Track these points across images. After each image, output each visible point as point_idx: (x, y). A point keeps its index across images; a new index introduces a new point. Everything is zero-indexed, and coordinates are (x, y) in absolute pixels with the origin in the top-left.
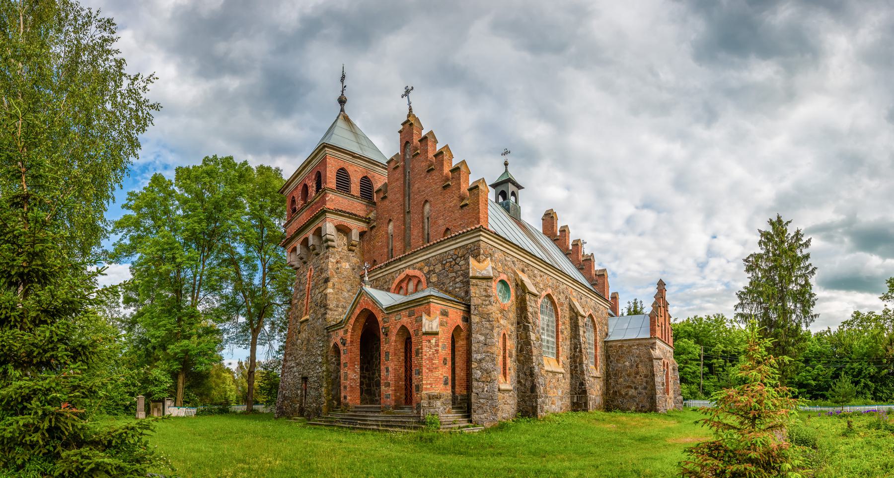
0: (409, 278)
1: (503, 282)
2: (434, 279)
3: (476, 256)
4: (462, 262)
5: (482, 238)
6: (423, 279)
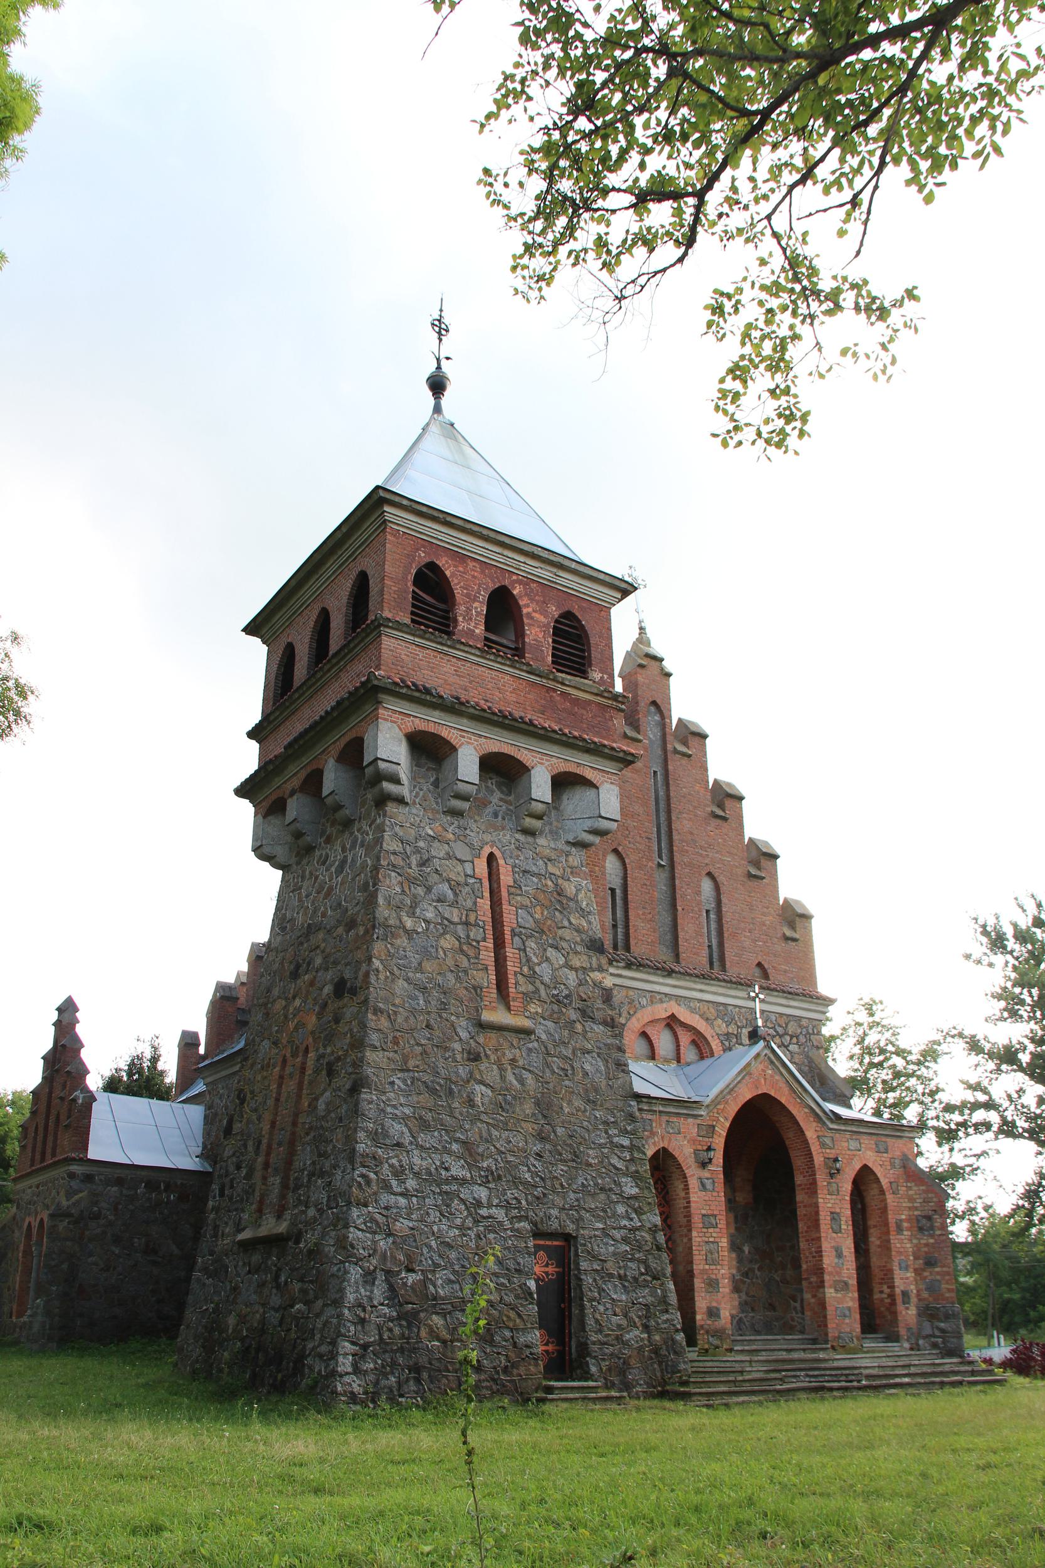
0: (672, 1023)
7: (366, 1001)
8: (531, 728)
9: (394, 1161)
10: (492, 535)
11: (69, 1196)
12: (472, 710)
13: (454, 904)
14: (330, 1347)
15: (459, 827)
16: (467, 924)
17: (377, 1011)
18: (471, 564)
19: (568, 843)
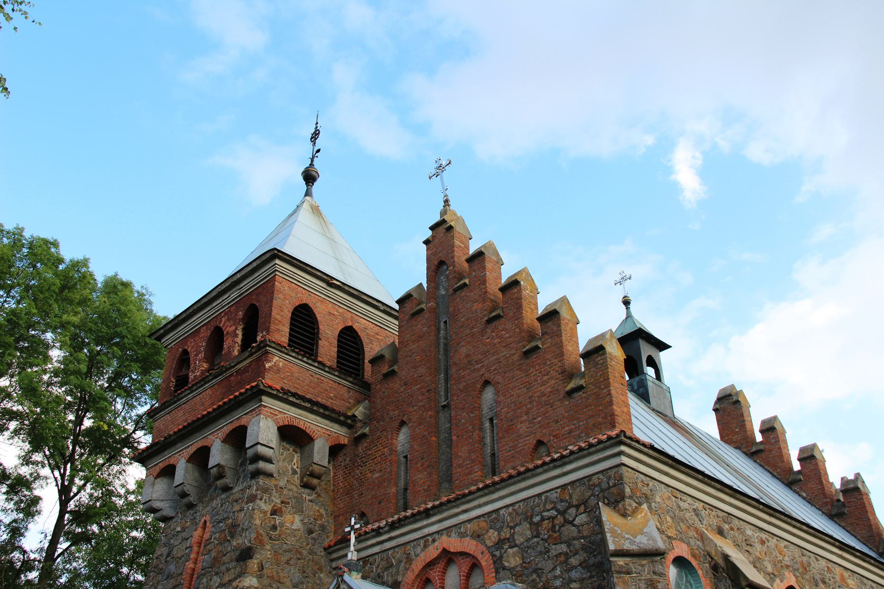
0: (448, 557)
1: (680, 562)
2: (513, 559)
3: (616, 501)
4: (582, 519)
5: (625, 460)
6: (485, 561)
8: (201, 421)
10: (198, 305)
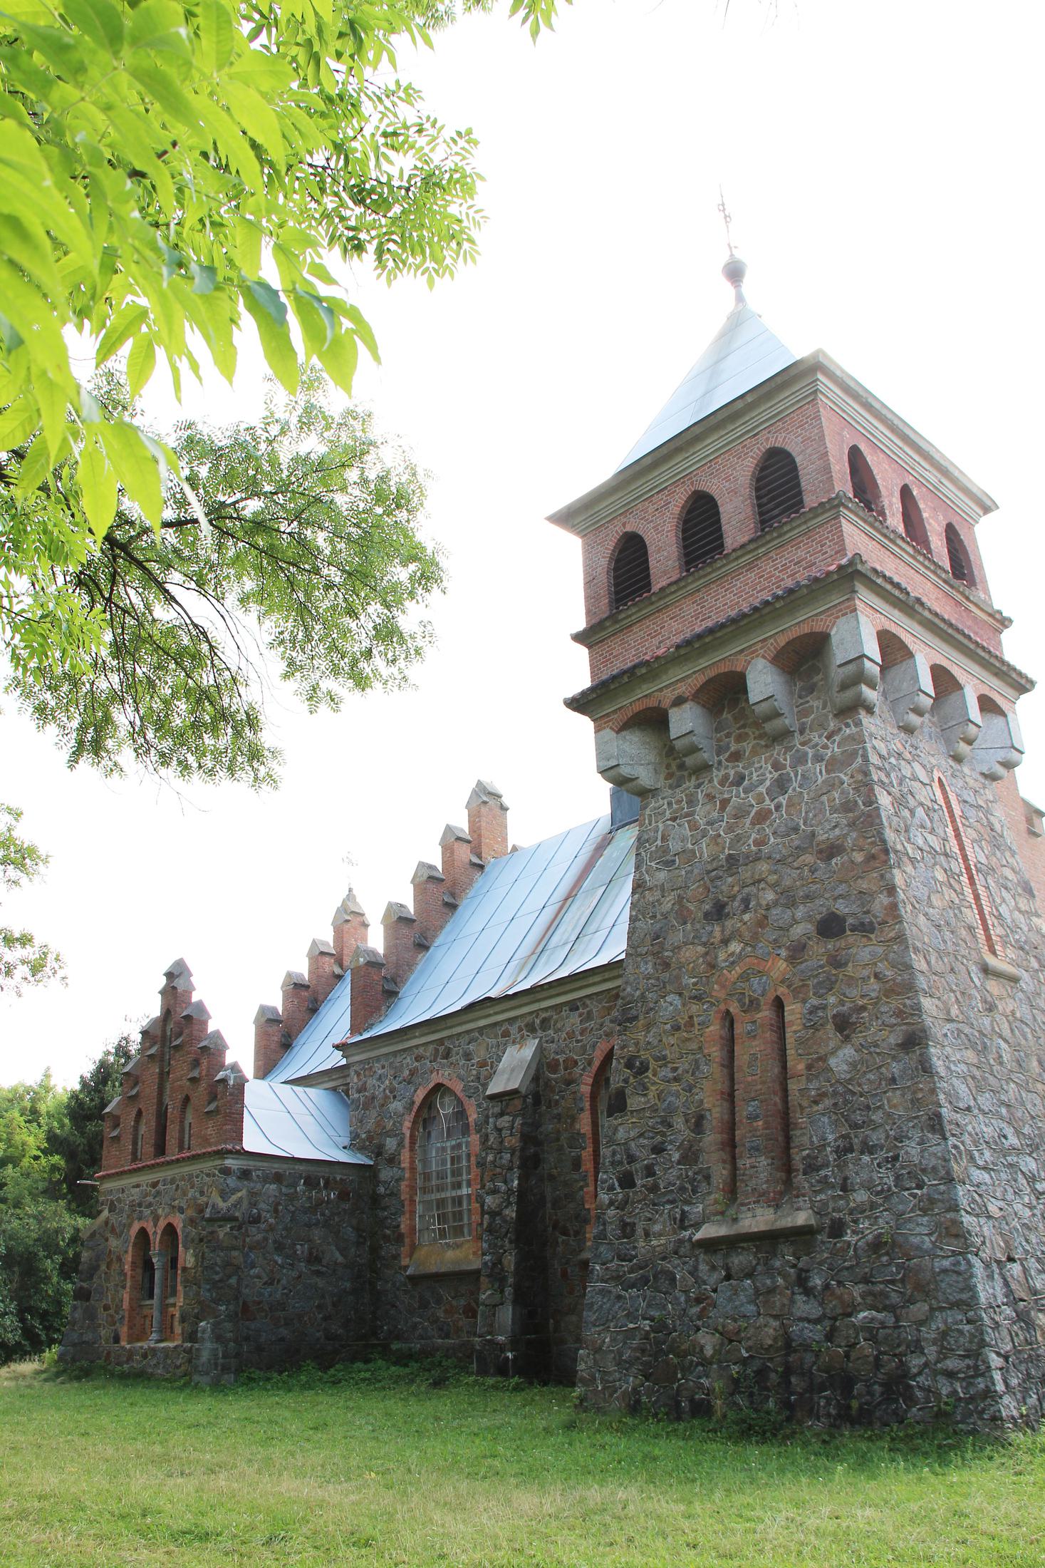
7: (901, 938)
8: (966, 641)
9: (969, 1128)
11: (224, 1195)
12: (926, 613)
13: (932, 831)
14: (967, 1361)
15: (912, 746)
16: (946, 855)
17: (916, 950)
18: (882, 456)
19: (982, 774)
